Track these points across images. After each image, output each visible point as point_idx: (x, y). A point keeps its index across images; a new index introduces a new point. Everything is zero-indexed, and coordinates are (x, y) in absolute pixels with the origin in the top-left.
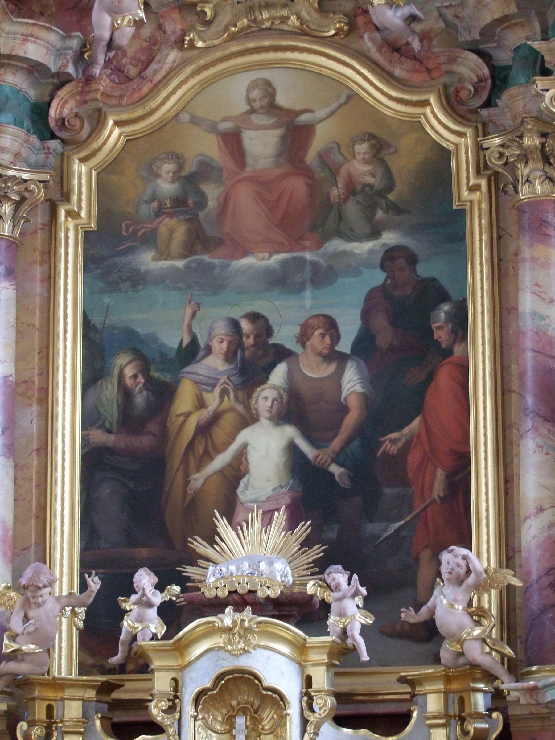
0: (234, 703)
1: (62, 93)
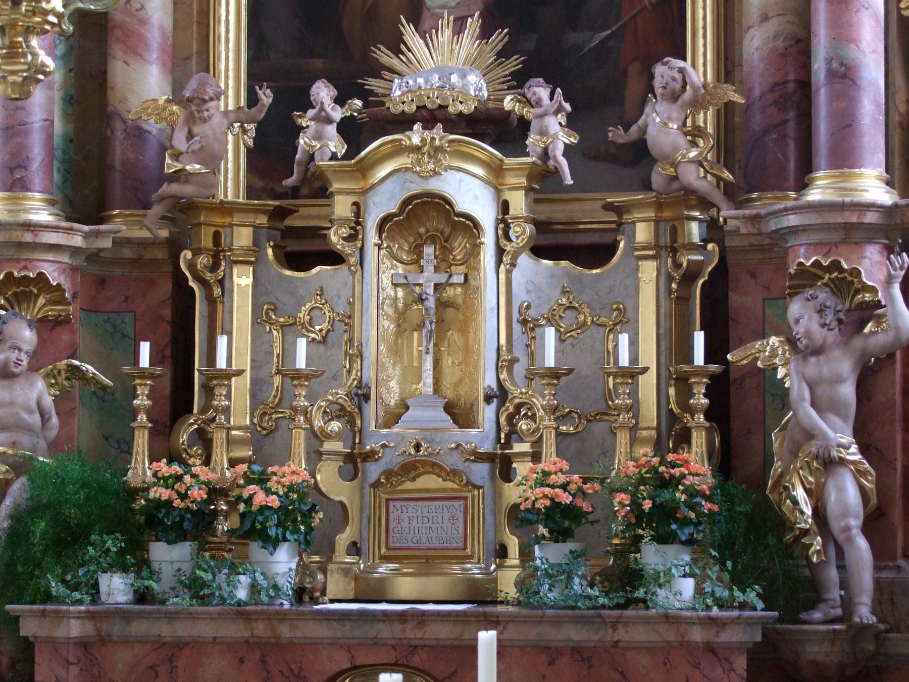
0: (422, 230)
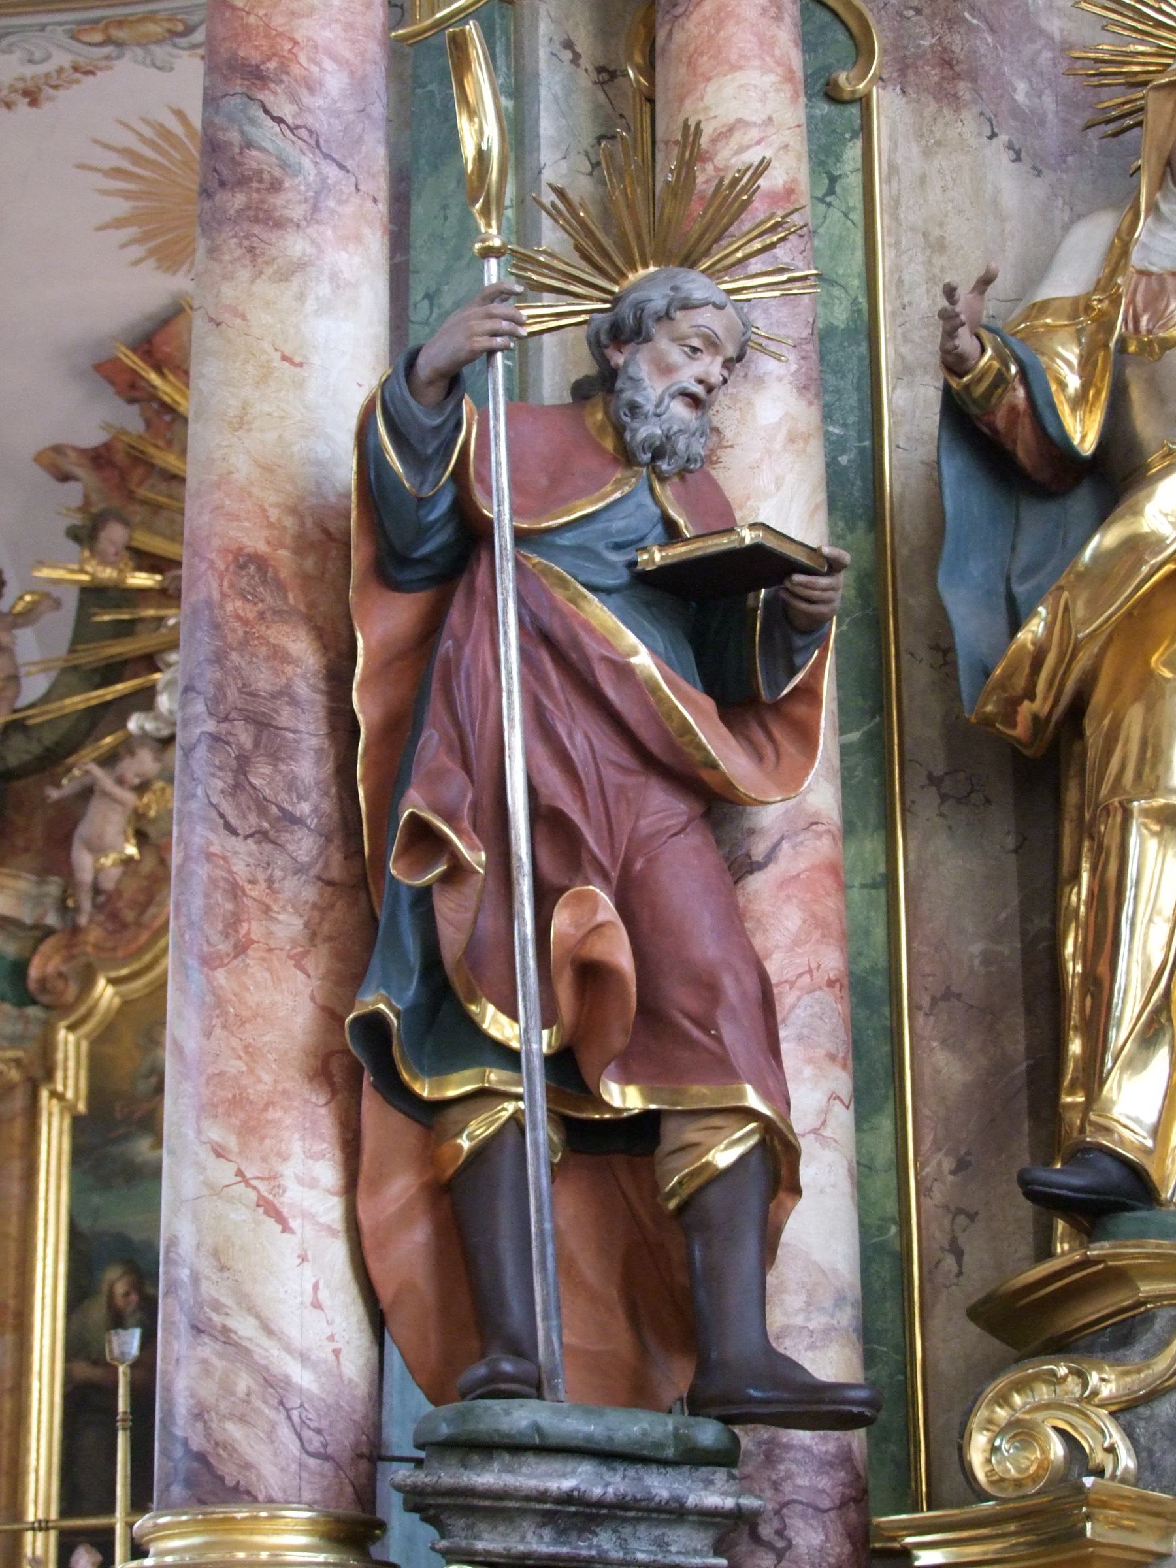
1: (46, 947)
